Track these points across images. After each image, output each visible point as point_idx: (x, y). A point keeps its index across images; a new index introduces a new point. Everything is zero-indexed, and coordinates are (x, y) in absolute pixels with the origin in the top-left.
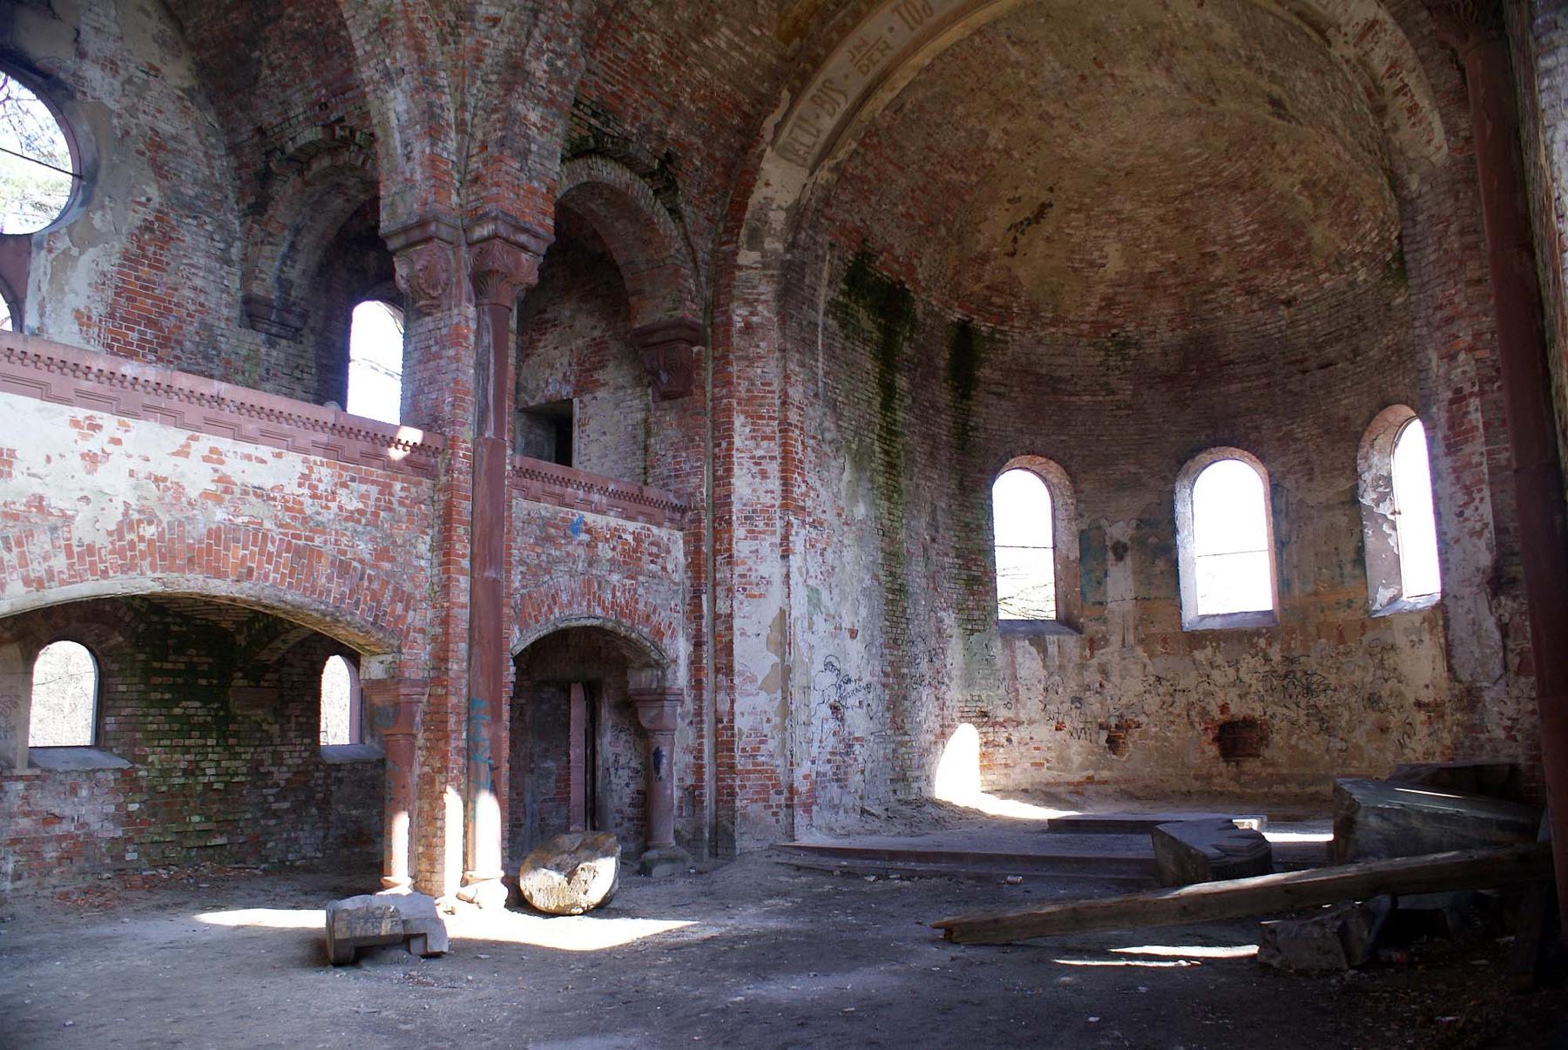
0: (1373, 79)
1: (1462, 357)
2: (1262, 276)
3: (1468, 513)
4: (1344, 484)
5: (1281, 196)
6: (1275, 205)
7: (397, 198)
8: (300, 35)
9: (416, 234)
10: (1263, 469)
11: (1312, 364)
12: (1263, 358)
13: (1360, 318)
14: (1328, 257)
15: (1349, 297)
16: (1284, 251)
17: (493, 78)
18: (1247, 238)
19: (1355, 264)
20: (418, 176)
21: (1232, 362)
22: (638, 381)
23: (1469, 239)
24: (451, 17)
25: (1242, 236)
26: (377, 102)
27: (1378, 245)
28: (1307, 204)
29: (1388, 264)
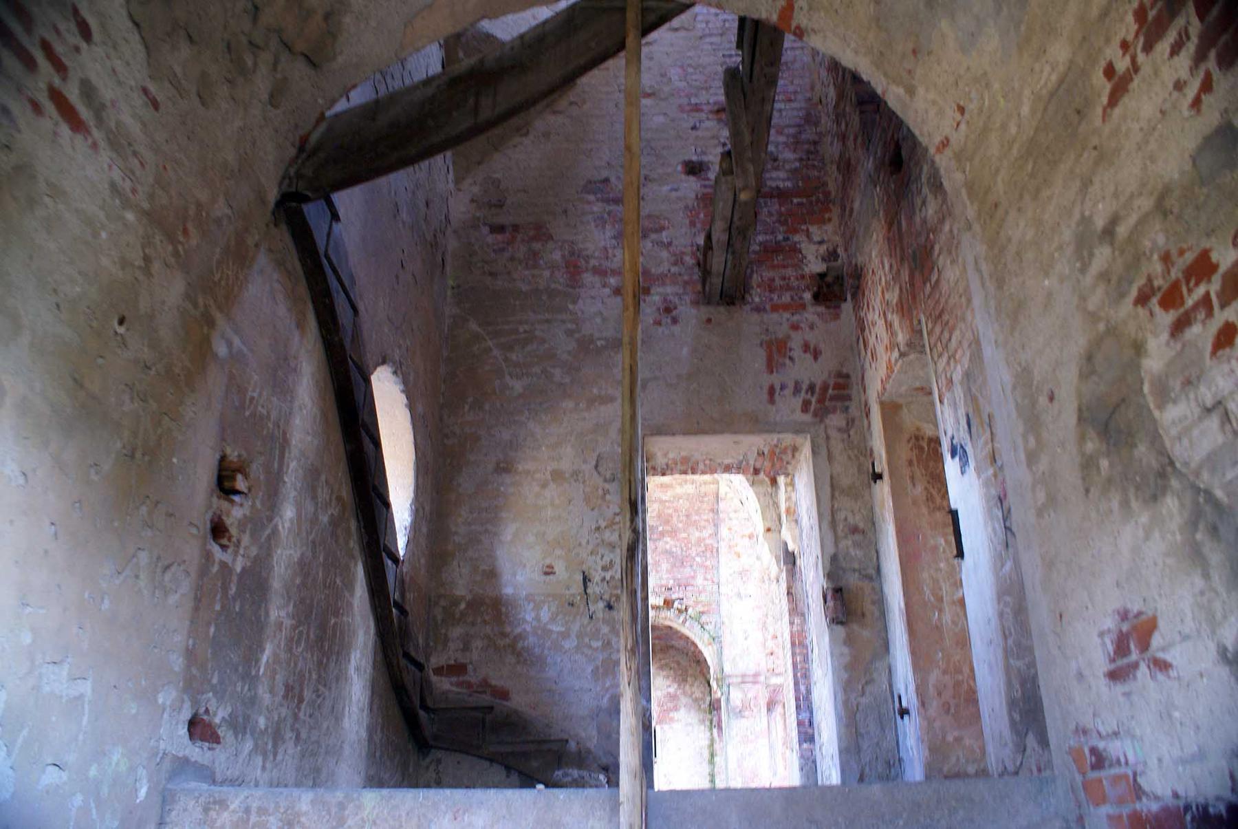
8: (668, 553)
9: (751, 679)
22: (702, 721)
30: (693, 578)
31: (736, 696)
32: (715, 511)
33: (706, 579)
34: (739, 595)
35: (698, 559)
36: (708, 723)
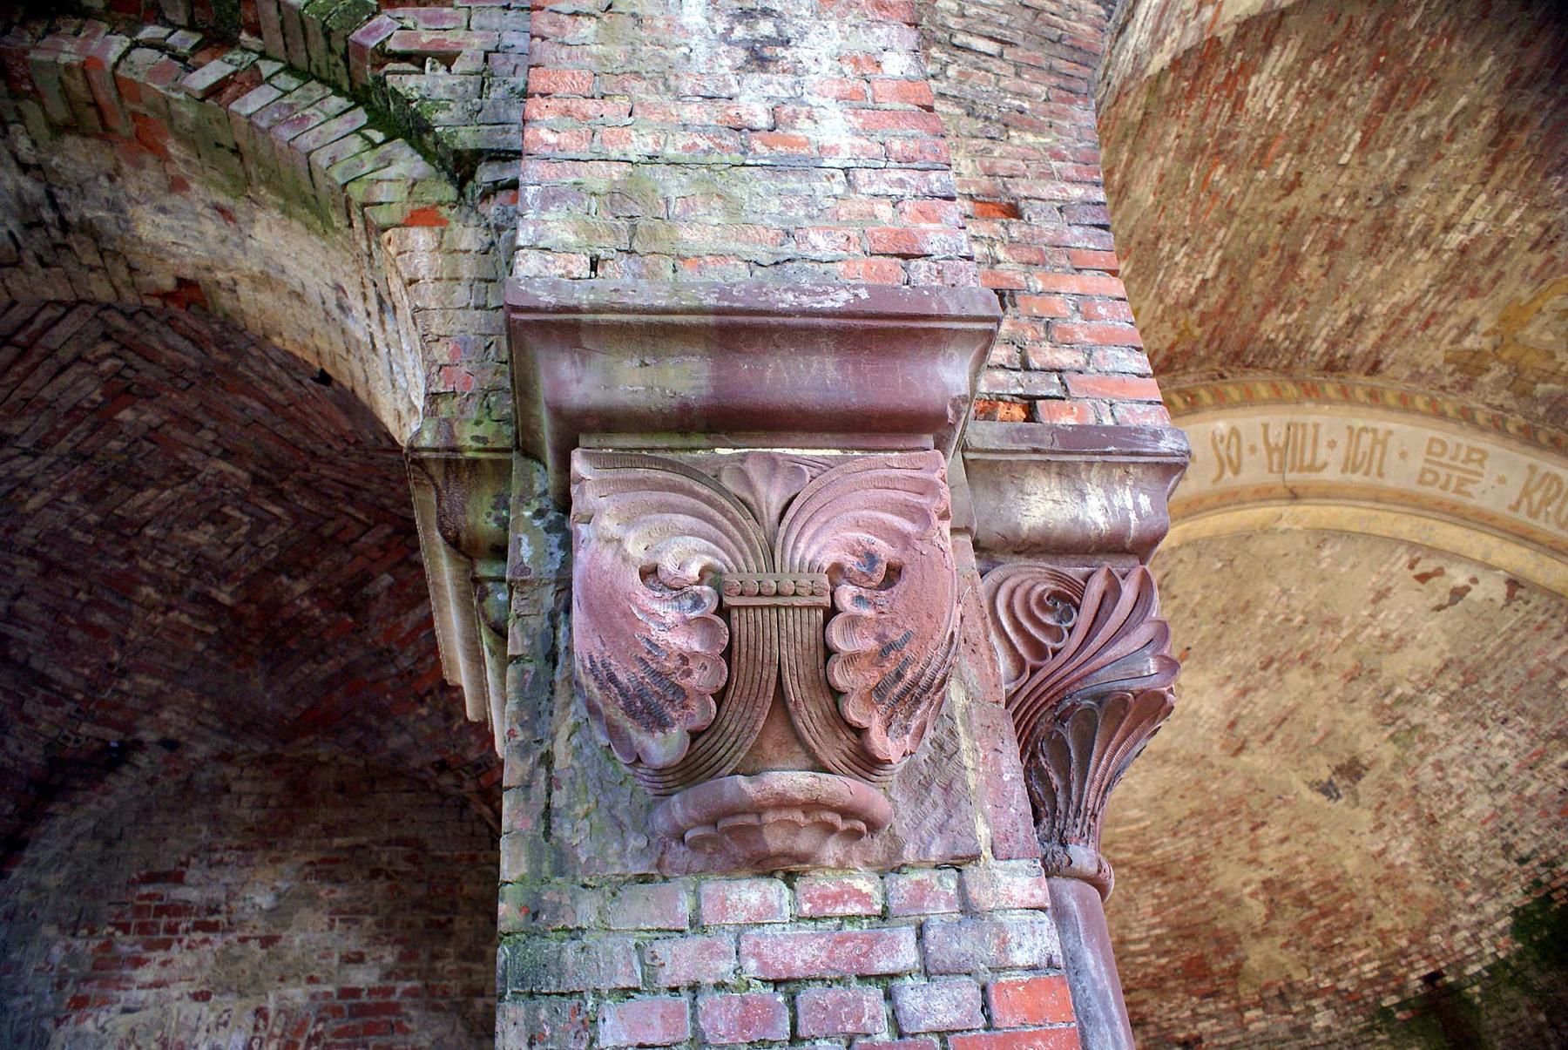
2: (1154, 1002)
5: (1220, 896)
6: (1204, 906)
14: (1268, 987)
16: (1196, 971)
18: (1145, 946)
19: (1315, 1003)
25: (1140, 941)
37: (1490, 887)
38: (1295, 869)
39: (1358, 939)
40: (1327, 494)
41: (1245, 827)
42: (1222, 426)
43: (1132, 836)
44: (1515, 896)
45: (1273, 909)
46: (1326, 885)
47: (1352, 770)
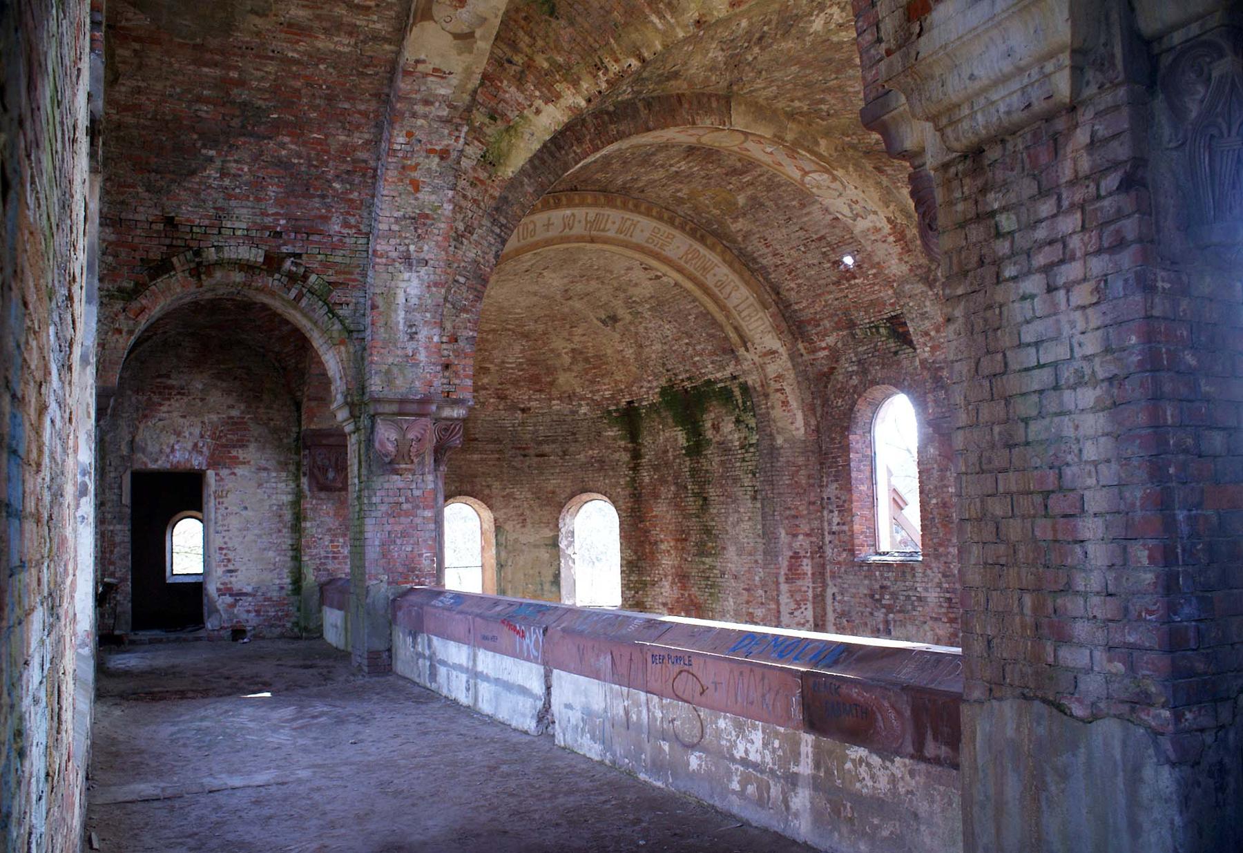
0: (765, 376)
1: (801, 537)
2: (512, 390)
3: (796, 613)
4: (548, 533)
5: (552, 351)
7: (395, 370)
8: (281, 164)
9: (413, 408)
10: (488, 515)
11: (532, 452)
12: (498, 441)
13: (574, 434)
15: (569, 418)
16: (534, 380)
17: (462, 280)
20: (422, 356)
21: (476, 439)
22: (283, 466)
23: (812, 481)
24: (461, 227)
26: (386, 276)
27: (607, 399)
28: (567, 360)
29: (609, 412)
30: (325, 219)
31: (387, 435)
32: (384, 98)
33: (346, 224)
34: (407, 259)
35: (337, 185)
36: (292, 468)
37: (657, 376)
38: (586, 347)
39: (606, 381)
40: (606, 241)
41: (568, 326)
42: (568, 212)
43: (517, 320)
44: (663, 382)
45: (574, 360)
46: (598, 357)
47: (614, 319)
